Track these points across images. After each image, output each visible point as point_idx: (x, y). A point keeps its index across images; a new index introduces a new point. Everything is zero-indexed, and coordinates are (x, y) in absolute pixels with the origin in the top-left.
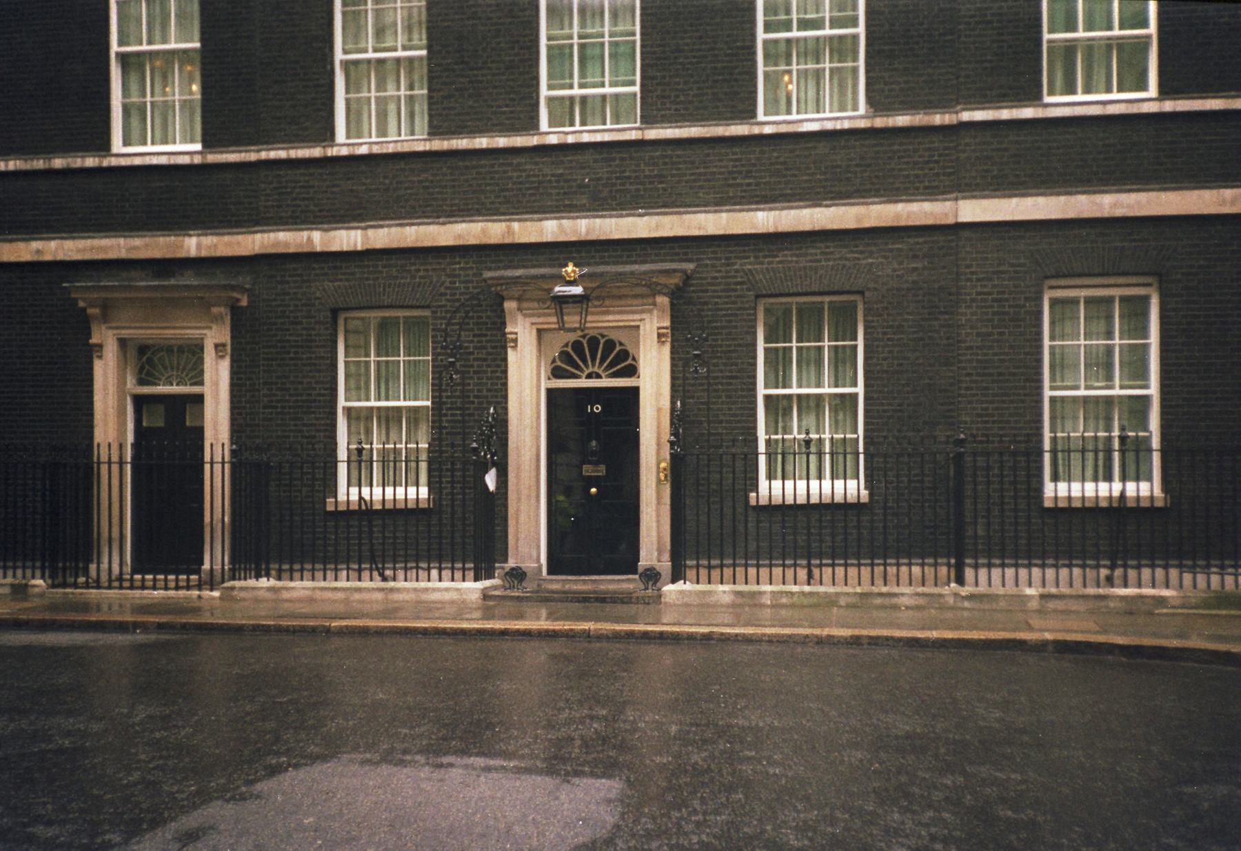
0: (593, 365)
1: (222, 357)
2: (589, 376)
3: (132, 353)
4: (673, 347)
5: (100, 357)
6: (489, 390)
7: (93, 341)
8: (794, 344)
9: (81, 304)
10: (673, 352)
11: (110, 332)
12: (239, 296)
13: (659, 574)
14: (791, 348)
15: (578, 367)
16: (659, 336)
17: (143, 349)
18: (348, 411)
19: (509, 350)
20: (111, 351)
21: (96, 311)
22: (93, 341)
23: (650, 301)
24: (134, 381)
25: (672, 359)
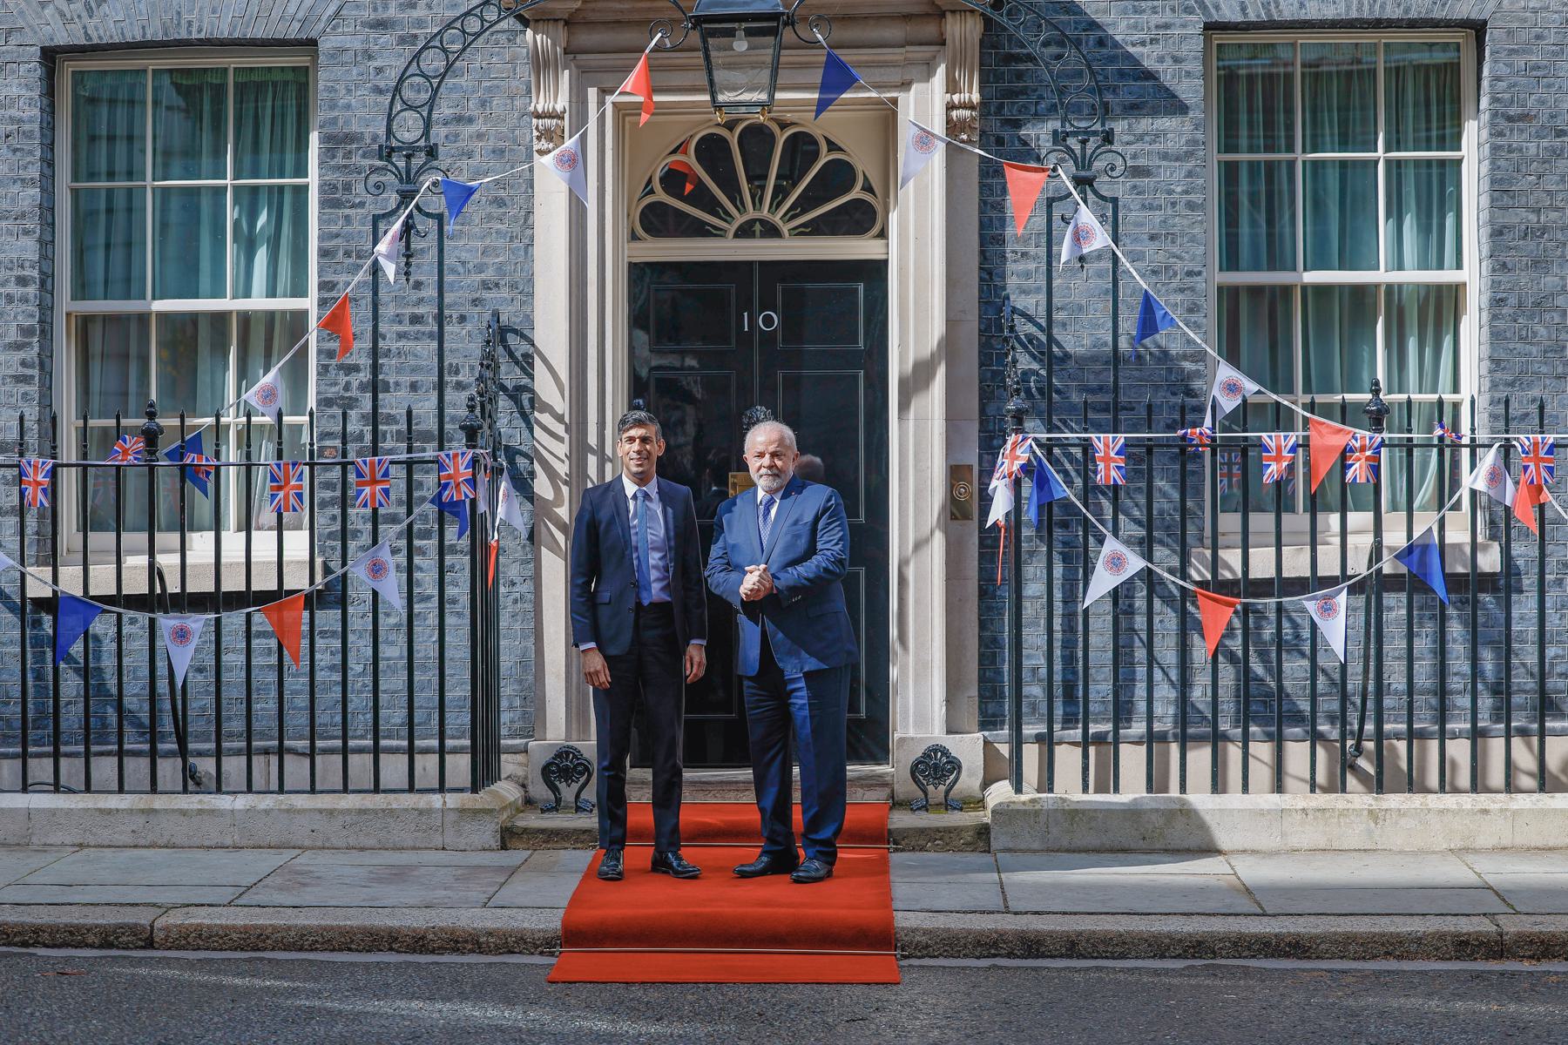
0: (757, 200)
2: (745, 232)
6: (480, 268)
8: (1300, 157)
13: (955, 766)
15: (713, 206)
18: (85, 324)
23: (930, 30)
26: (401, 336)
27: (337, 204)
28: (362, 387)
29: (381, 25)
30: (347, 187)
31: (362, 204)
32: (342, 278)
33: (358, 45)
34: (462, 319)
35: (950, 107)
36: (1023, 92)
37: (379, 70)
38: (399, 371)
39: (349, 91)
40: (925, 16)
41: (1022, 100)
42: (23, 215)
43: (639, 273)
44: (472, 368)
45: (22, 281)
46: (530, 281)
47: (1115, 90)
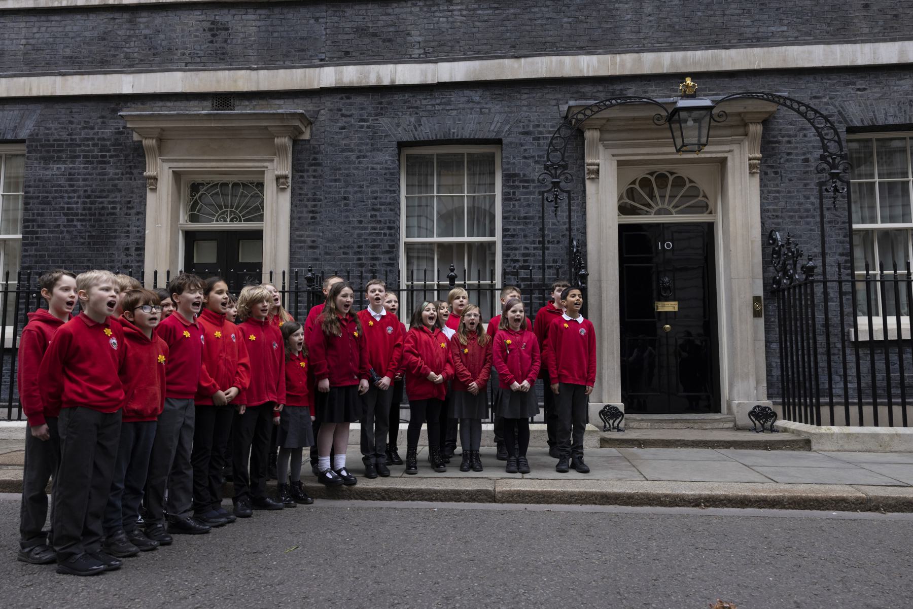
1: (283, 190)
3: (186, 191)
4: (761, 180)
5: (154, 190)
7: (149, 172)
8: (877, 180)
9: (136, 137)
10: (763, 185)
11: (166, 166)
12: (304, 129)
14: (874, 183)
16: (751, 166)
17: (195, 187)
19: (588, 183)
20: (166, 184)
21: (153, 142)
22: (149, 172)
23: (741, 130)
24: (186, 218)
25: (762, 191)
26: (535, 249)
27: (510, 200)
28: (522, 267)
29: (527, 133)
30: (514, 193)
31: (520, 200)
32: (512, 227)
33: (517, 141)
34: (558, 242)
35: (750, 159)
36: (775, 155)
37: (525, 150)
38: (535, 262)
39: (514, 158)
40: (737, 126)
41: (774, 158)
42: (390, 204)
43: (622, 228)
44: (562, 261)
45: (390, 228)
46: (585, 227)
47: (811, 153)
